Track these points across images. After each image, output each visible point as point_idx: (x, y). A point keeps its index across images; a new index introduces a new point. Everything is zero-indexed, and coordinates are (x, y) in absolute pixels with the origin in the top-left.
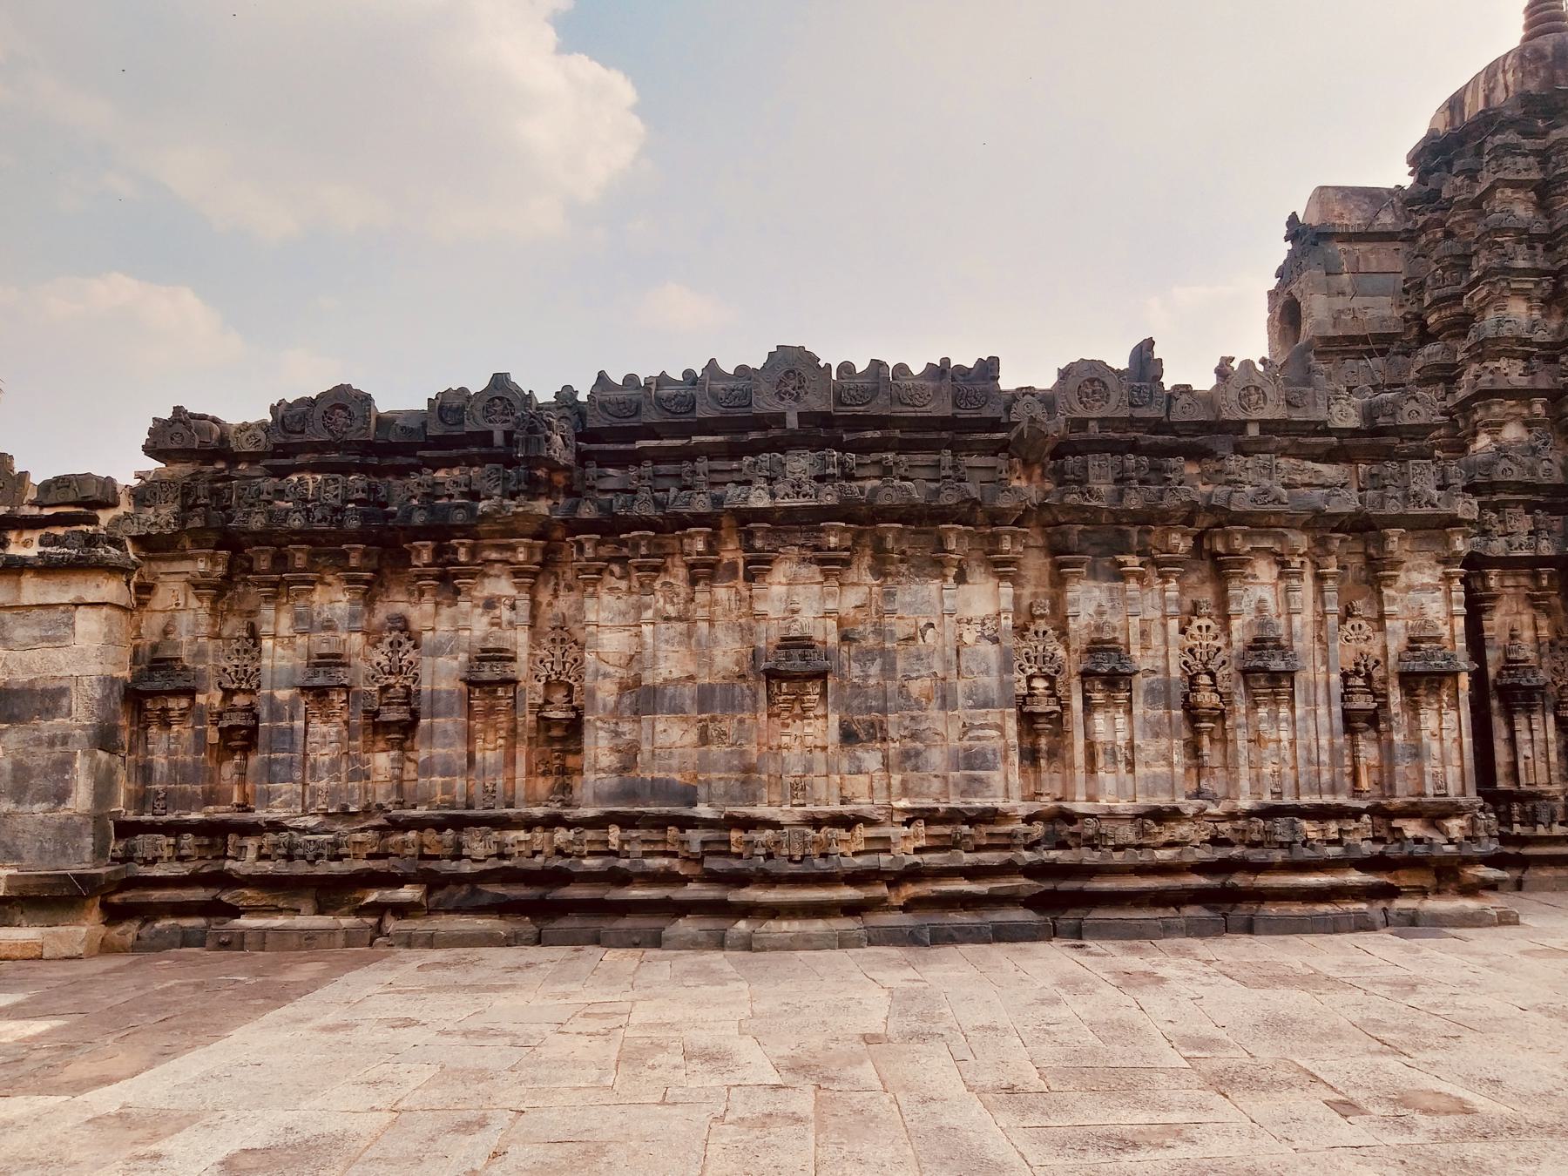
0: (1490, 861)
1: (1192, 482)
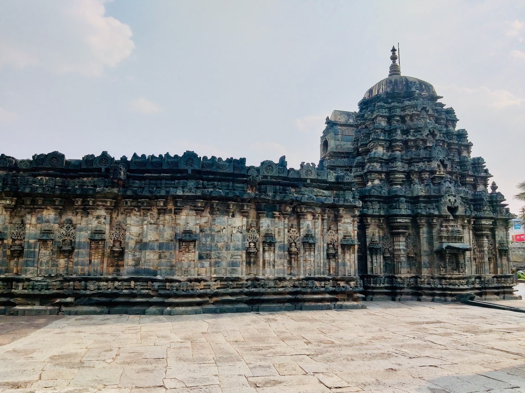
0: (360, 292)
1: (293, 194)
